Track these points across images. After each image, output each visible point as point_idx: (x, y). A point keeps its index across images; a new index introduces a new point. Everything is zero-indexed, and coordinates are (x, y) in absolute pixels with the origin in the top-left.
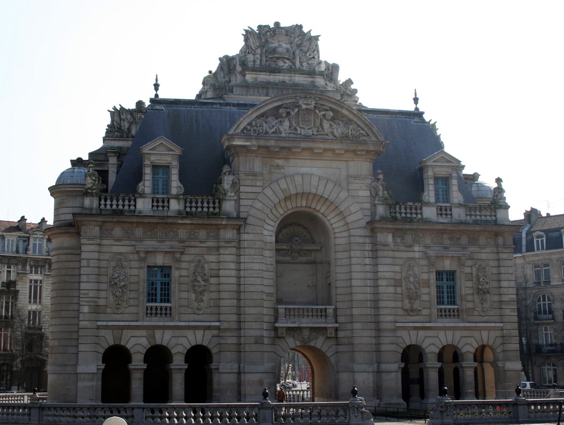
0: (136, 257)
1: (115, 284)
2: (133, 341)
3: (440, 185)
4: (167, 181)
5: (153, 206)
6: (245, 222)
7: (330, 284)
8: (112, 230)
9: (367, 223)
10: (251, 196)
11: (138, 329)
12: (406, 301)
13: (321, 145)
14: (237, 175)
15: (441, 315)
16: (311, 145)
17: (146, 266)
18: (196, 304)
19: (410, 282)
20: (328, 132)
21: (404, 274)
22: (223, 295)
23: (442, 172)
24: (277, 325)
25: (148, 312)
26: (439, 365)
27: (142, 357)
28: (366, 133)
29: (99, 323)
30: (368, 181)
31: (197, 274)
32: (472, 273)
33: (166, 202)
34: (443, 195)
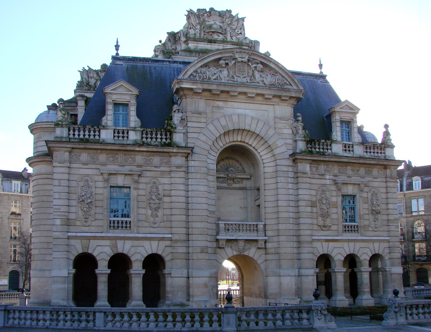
0: (100, 178)
1: (83, 201)
2: (99, 249)
3: (344, 128)
4: (126, 117)
5: (114, 137)
6: (192, 150)
7: (259, 206)
8: (80, 156)
9: (290, 155)
10: (196, 130)
11: (103, 240)
12: (320, 219)
13: (254, 91)
14: (185, 113)
15: (345, 231)
16: (245, 90)
17: (109, 186)
18: (152, 219)
19: (323, 203)
20: (259, 80)
21: (319, 198)
22: (175, 212)
23: (346, 117)
24: (218, 237)
25: (111, 225)
26: (370, 269)
27: (106, 263)
28: (289, 82)
29: (70, 234)
30: (291, 122)
31: (152, 194)
32: (368, 198)
33: (126, 133)
34: (346, 135)
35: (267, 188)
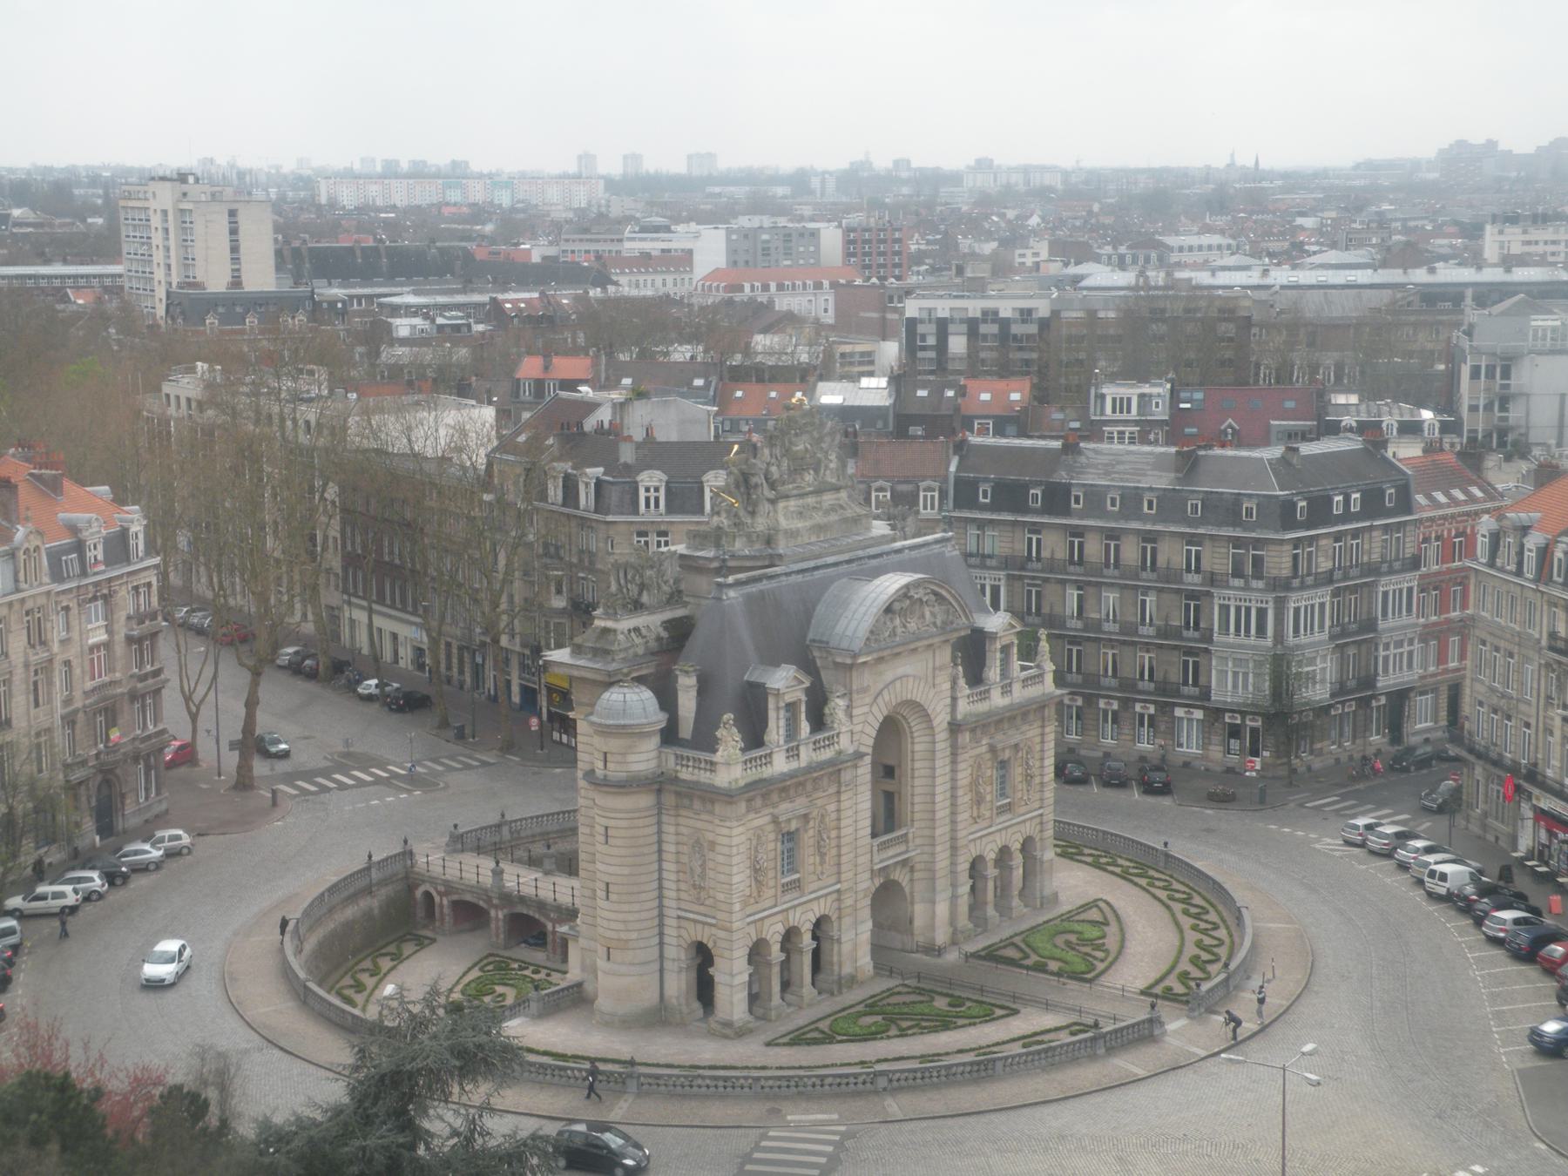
35: (917, 773)
